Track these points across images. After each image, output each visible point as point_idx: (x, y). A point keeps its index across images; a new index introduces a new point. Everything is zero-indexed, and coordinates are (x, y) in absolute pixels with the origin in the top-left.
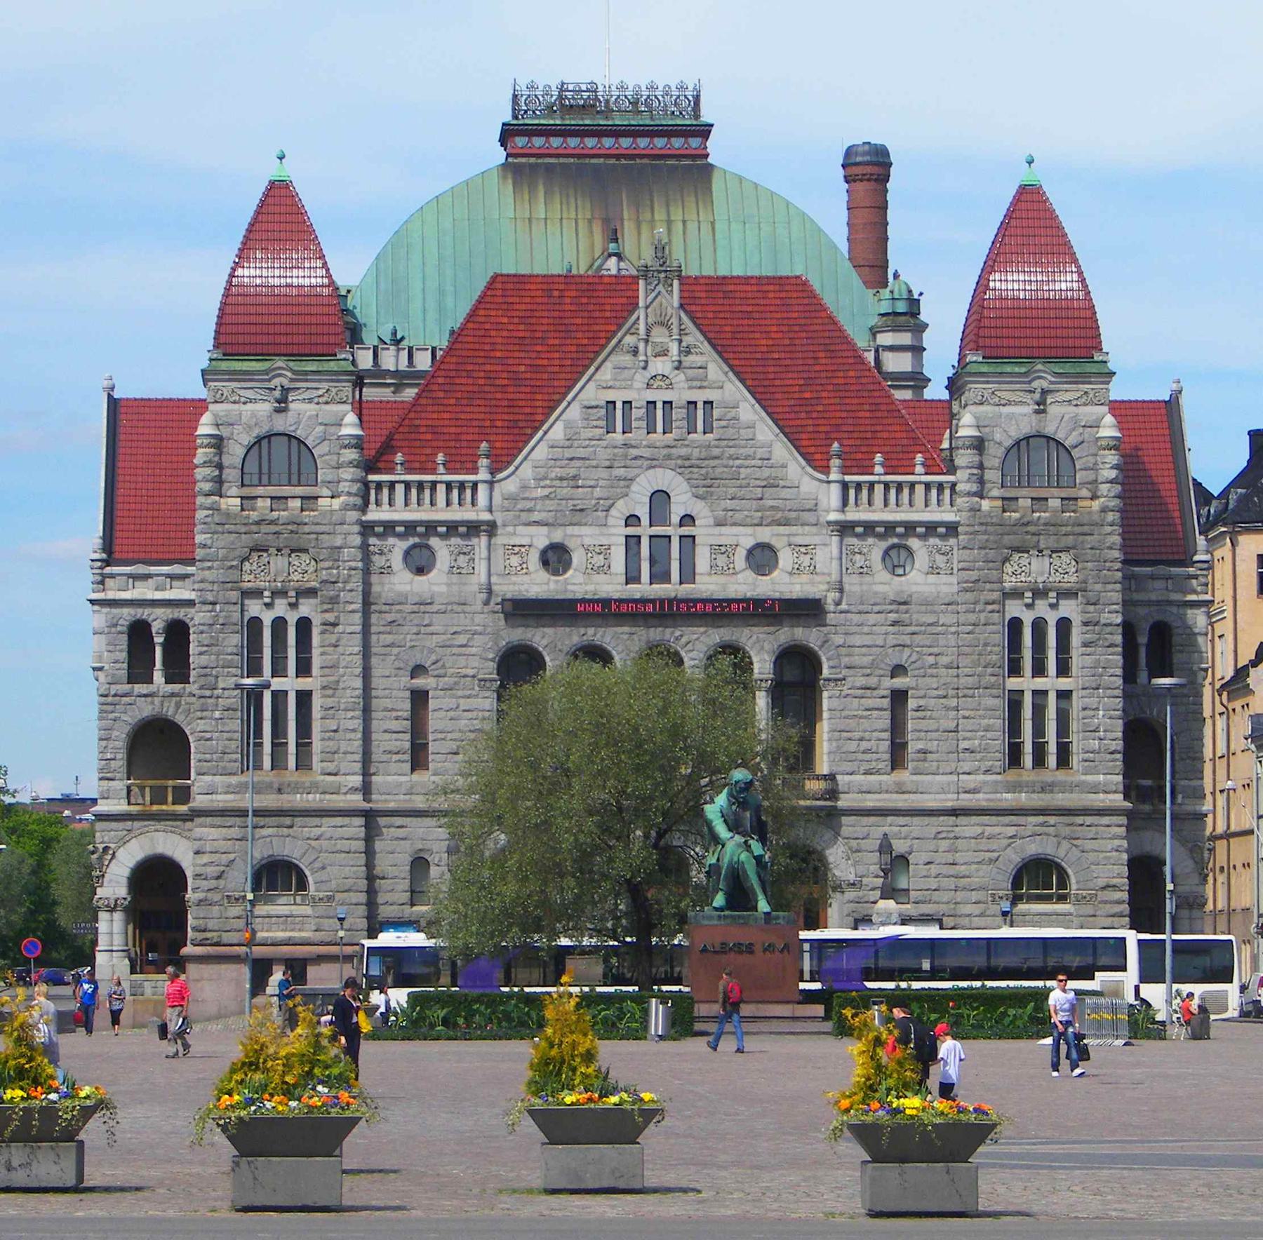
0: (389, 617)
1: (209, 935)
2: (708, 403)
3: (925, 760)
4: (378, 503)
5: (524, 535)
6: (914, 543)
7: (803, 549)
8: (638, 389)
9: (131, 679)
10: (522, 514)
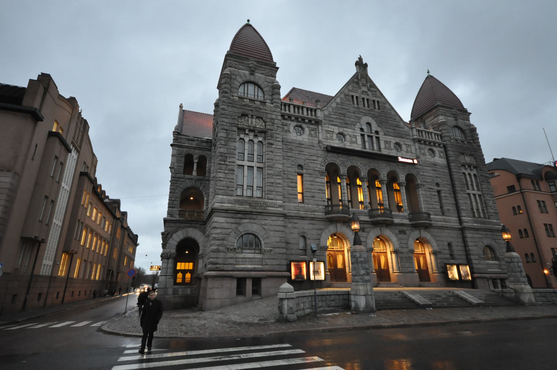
0: (290, 147)
1: (218, 266)
2: (378, 102)
3: (449, 212)
4: (285, 110)
5: (331, 128)
6: (435, 149)
7: (408, 146)
8: (360, 94)
9: (185, 173)
10: (330, 122)
